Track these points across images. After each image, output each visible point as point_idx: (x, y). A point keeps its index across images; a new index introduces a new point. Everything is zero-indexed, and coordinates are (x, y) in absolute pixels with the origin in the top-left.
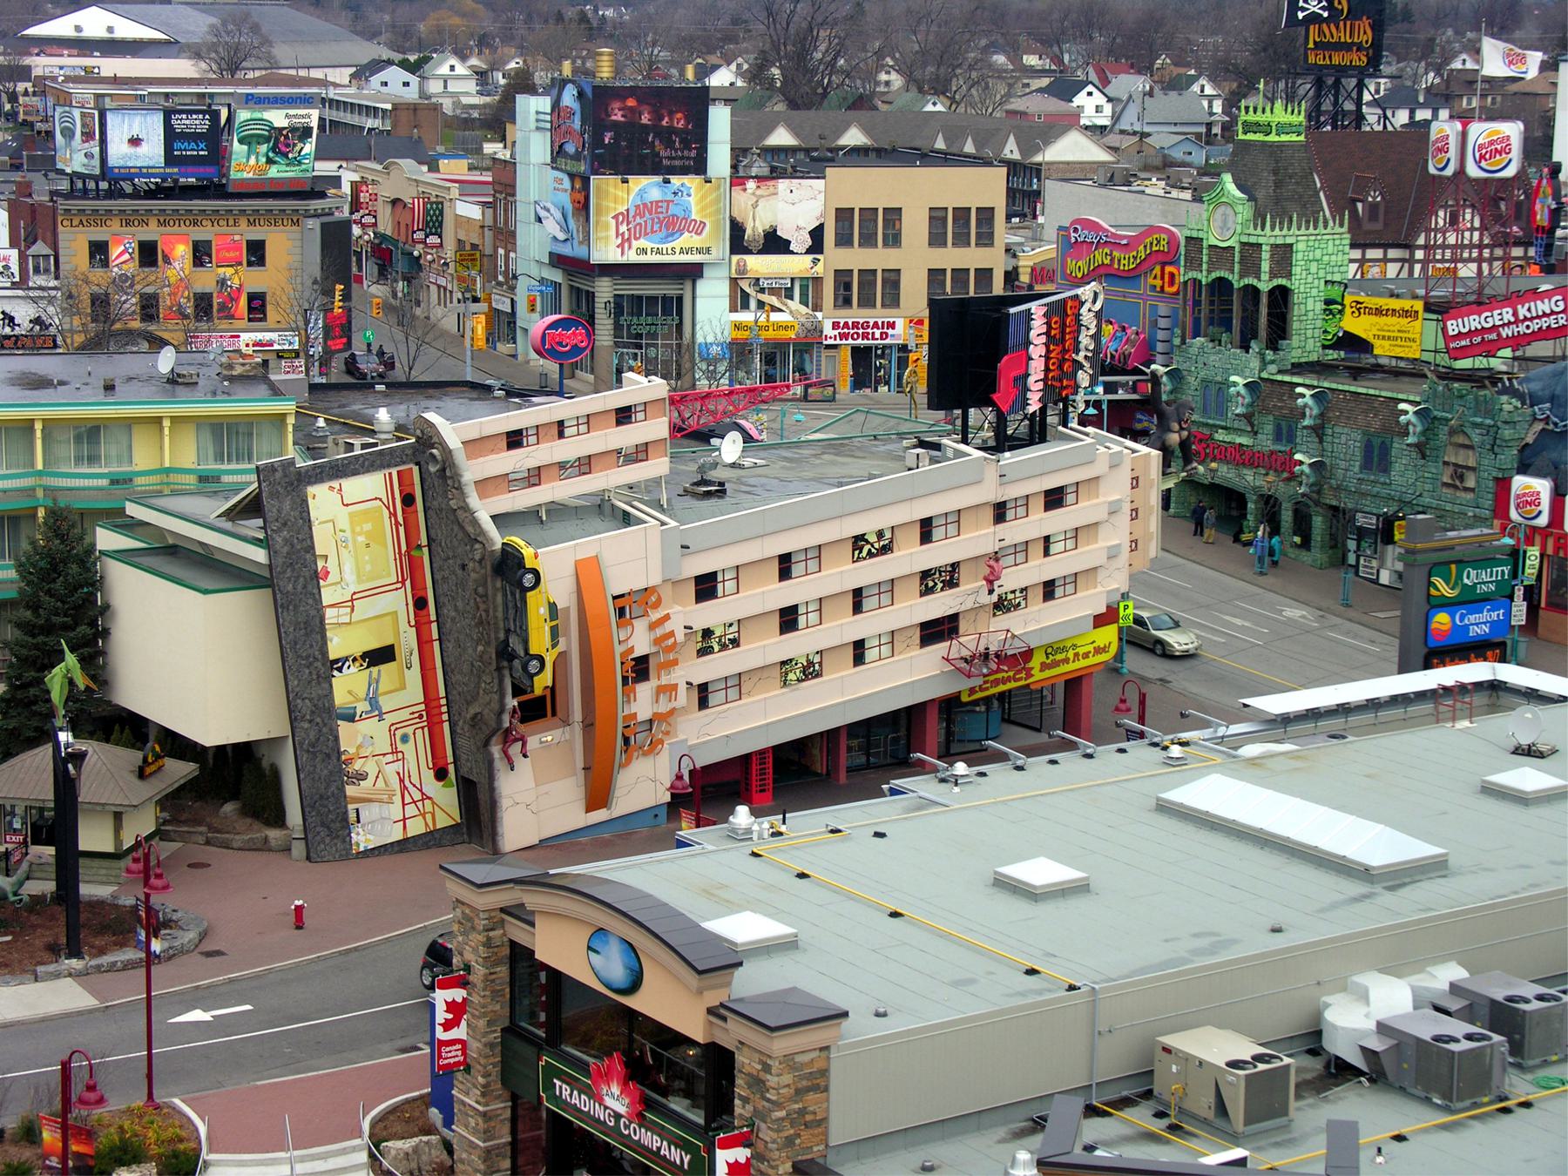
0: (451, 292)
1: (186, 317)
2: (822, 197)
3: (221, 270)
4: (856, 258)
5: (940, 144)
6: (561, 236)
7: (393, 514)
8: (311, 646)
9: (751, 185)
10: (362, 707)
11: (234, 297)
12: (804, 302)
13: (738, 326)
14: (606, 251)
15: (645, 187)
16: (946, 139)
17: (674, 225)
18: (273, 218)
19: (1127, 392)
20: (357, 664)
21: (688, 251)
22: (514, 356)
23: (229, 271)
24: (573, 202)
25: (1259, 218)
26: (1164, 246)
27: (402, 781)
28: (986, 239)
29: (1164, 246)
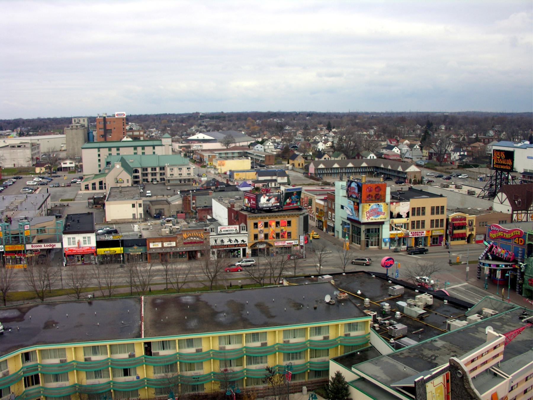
0: (314, 218)
1: (274, 238)
2: (409, 206)
3: (282, 228)
4: (416, 218)
5: (382, 166)
6: (351, 214)
7: (445, 386)
9: (394, 204)
11: (284, 233)
12: (405, 228)
13: (391, 234)
14: (364, 219)
15: (373, 205)
16: (384, 165)
17: (378, 213)
18: (293, 216)
19: (510, 267)
21: (382, 219)
22: (334, 235)
23: (283, 228)
24: (355, 208)
26: (519, 233)
28: (442, 213)
29: (519, 233)
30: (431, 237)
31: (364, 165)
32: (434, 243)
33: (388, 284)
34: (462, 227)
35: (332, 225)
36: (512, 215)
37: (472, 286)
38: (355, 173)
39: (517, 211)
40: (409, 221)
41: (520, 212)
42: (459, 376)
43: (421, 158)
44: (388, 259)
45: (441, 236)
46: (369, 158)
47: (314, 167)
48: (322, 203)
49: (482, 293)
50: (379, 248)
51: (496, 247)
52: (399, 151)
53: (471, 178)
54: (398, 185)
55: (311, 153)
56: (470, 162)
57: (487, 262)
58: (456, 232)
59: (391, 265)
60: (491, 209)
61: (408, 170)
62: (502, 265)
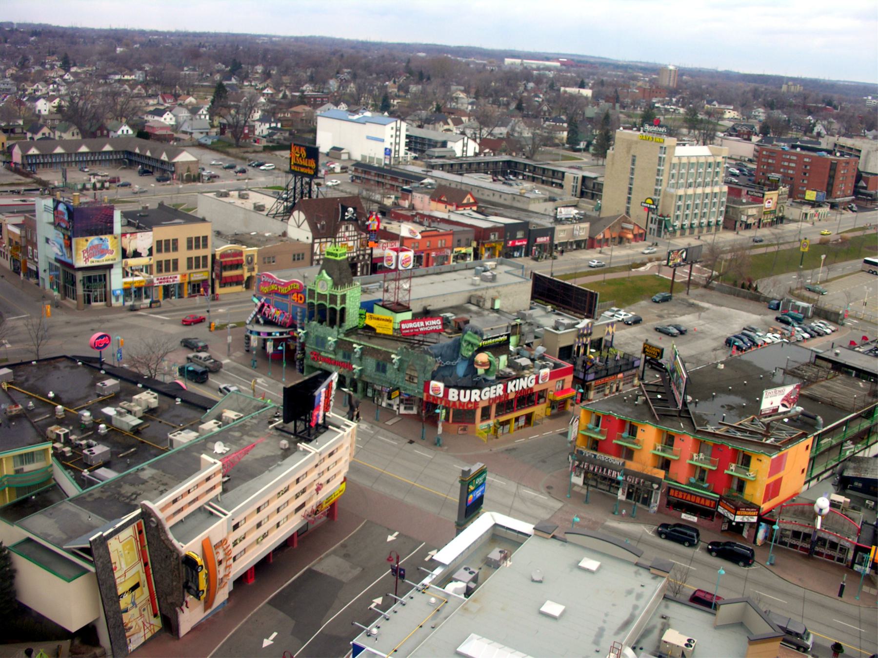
4: (164, 256)
5: (137, 151)
6: (60, 254)
9: (128, 236)
12: (147, 272)
13: (125, 283)
15: (94, 240)
17: (103, 252)
22: (38, 284)
25: (335, 285)
28: (205, 246)
29: (298, 287)
30: (189, 283)
31: (108, 148)
32: (194, 291)
33: (98, 375)
34: (238, 265)
35: (34, 268)
36: (312, 245)
37: (235, 364)
38: (92, 161)
39: (320, 238)
40: (153, 261)
41: (324, 240)
42: (153, 525)
43: (207, 133)
44: (101, 337)
45: (205, 281)
46: (120, 132)
47: (20, 152)
48: (17, 231)
49: (248, 374)
50: (107, 305)
51: (269, 307)
52: (174, 119)
53: (279, 169)
54: (161, 183)
55: (21, 122)
56: (285, 139)
57: (257, 328)
58: (226, 274)
59: (106, 345)
60: (285, 234)
61: (175, 160)
62: (276, 332)
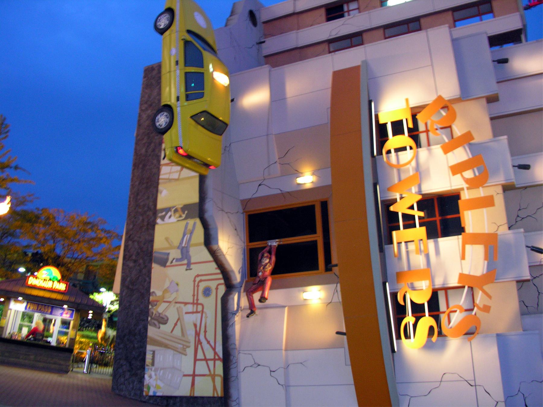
8: (148, 198)
10: (175, 254)
20: (177, 215)
27: (197, 334)
